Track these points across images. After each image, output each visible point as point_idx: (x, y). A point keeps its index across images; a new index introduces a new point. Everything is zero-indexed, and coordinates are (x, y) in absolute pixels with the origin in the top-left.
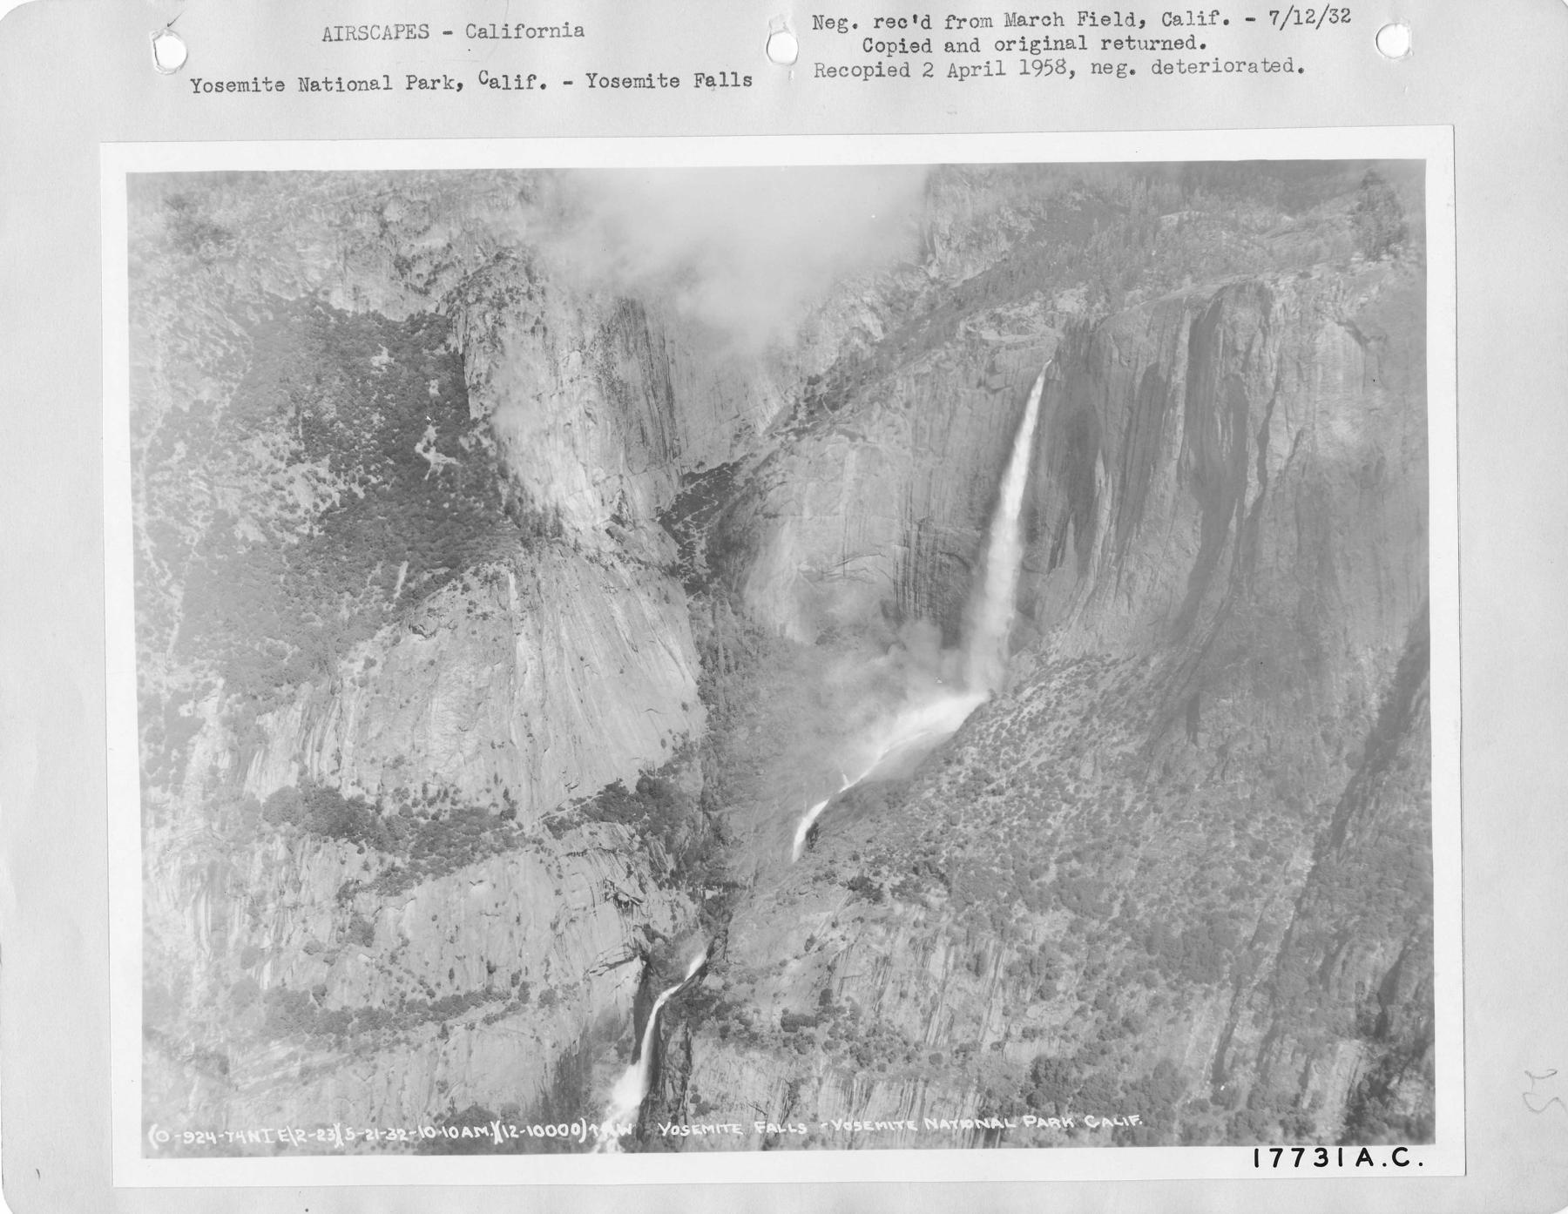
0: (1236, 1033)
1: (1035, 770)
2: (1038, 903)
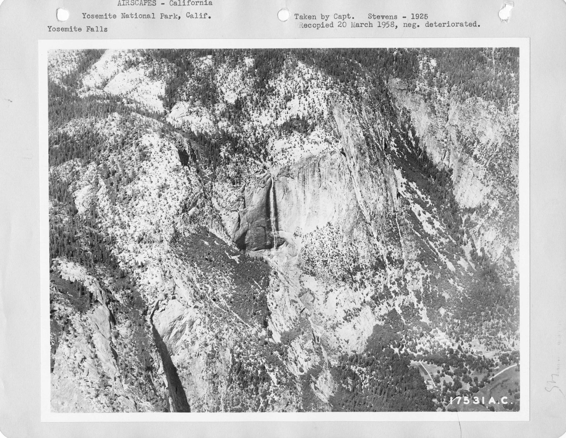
2: (355, 274)
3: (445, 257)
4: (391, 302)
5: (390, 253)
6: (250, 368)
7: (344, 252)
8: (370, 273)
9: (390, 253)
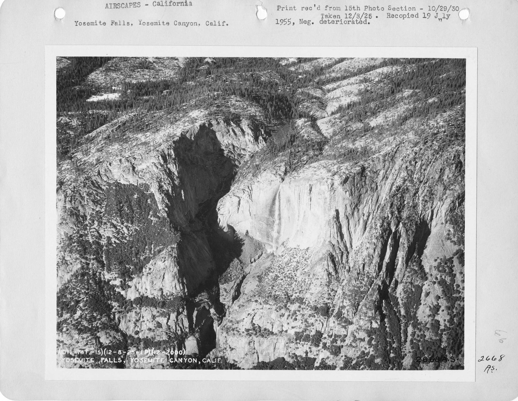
1: (288, 275)
2: (292, 303)
3: (411, 351)
4: (314, 349)
5: (343, 307)
6: (69, 296)
7: (299, 279)
8: (308, 312)
9: (343, 307)
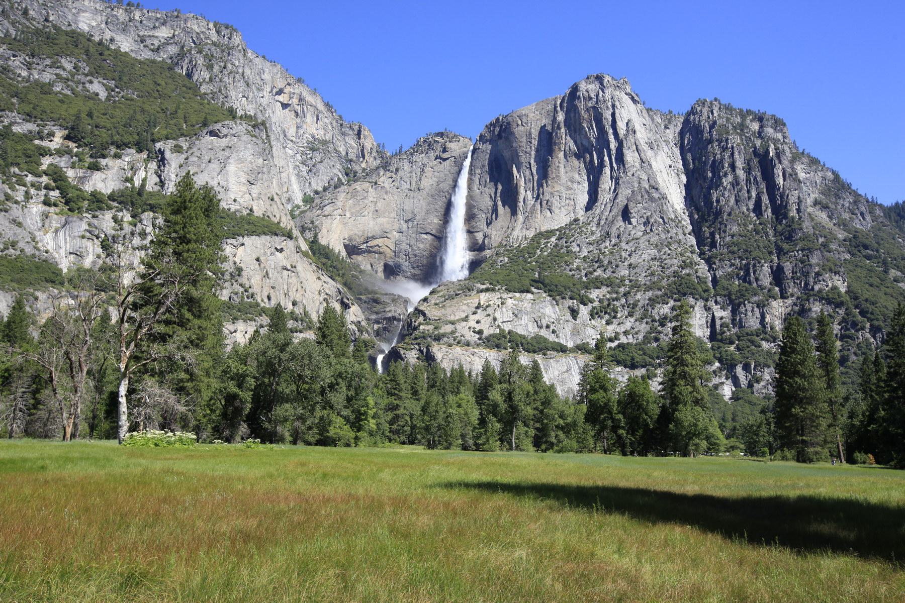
0: (716, 314)
